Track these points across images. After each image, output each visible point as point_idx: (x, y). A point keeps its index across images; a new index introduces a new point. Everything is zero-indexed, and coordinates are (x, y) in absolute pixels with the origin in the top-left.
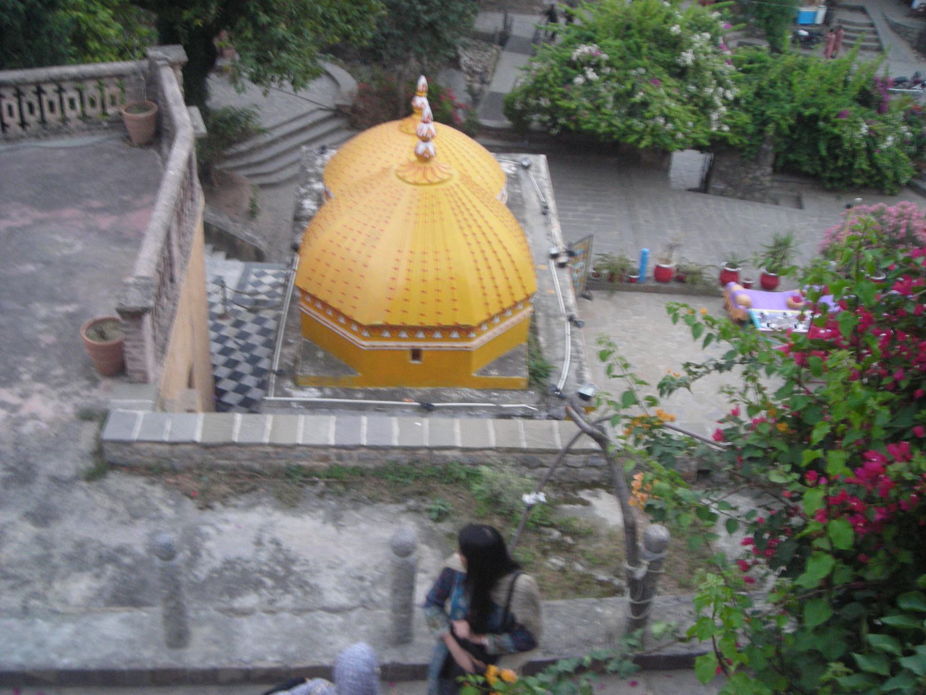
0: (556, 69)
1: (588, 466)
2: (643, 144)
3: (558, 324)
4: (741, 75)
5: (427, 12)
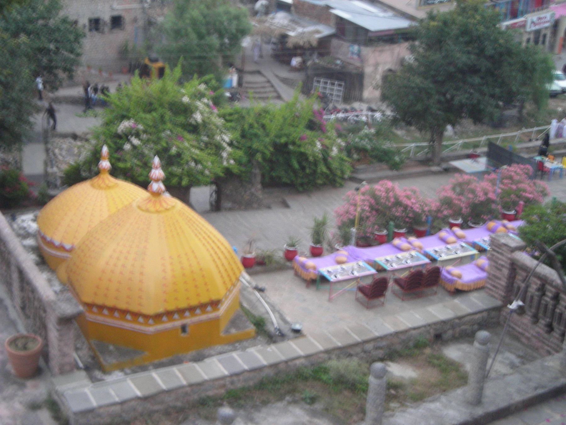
1: (377, 348)
4: (229, 124)
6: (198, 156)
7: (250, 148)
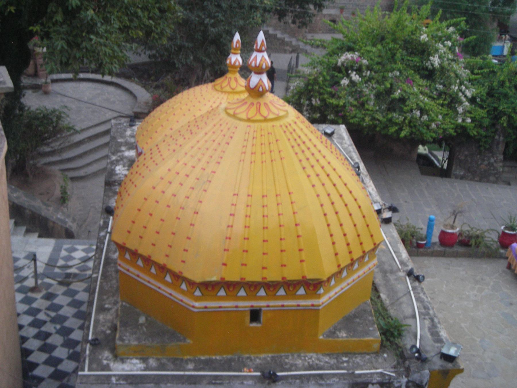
0: (325, 73)
2: (403, 134)
3: (396, 280)
5: (213, 25)
6: (425, 104)
7: (495, 109)
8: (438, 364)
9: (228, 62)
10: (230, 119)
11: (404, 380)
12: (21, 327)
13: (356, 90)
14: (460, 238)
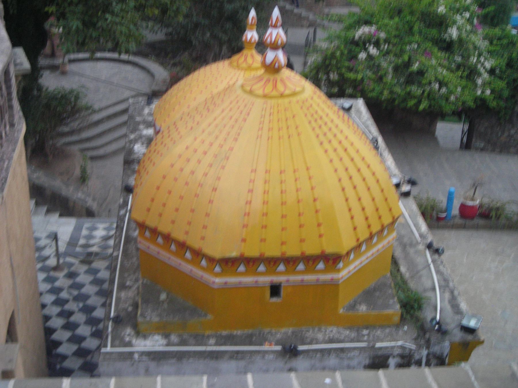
2: (421, 107)
8: (458, 336)
9: (244, 38)
10: (246, 96)
11: (425, 352)
12: (44, 306)
13: (374, 64)
14: (480, 211)
